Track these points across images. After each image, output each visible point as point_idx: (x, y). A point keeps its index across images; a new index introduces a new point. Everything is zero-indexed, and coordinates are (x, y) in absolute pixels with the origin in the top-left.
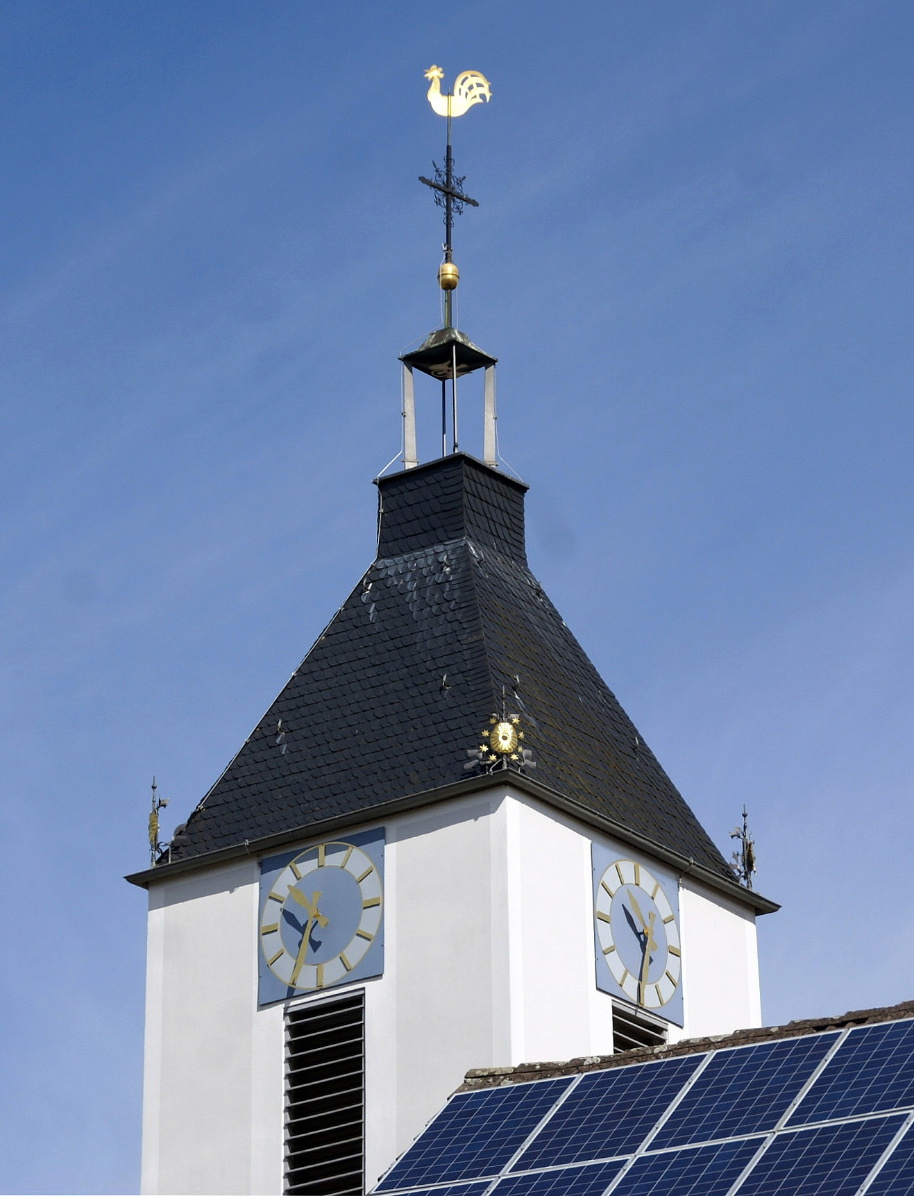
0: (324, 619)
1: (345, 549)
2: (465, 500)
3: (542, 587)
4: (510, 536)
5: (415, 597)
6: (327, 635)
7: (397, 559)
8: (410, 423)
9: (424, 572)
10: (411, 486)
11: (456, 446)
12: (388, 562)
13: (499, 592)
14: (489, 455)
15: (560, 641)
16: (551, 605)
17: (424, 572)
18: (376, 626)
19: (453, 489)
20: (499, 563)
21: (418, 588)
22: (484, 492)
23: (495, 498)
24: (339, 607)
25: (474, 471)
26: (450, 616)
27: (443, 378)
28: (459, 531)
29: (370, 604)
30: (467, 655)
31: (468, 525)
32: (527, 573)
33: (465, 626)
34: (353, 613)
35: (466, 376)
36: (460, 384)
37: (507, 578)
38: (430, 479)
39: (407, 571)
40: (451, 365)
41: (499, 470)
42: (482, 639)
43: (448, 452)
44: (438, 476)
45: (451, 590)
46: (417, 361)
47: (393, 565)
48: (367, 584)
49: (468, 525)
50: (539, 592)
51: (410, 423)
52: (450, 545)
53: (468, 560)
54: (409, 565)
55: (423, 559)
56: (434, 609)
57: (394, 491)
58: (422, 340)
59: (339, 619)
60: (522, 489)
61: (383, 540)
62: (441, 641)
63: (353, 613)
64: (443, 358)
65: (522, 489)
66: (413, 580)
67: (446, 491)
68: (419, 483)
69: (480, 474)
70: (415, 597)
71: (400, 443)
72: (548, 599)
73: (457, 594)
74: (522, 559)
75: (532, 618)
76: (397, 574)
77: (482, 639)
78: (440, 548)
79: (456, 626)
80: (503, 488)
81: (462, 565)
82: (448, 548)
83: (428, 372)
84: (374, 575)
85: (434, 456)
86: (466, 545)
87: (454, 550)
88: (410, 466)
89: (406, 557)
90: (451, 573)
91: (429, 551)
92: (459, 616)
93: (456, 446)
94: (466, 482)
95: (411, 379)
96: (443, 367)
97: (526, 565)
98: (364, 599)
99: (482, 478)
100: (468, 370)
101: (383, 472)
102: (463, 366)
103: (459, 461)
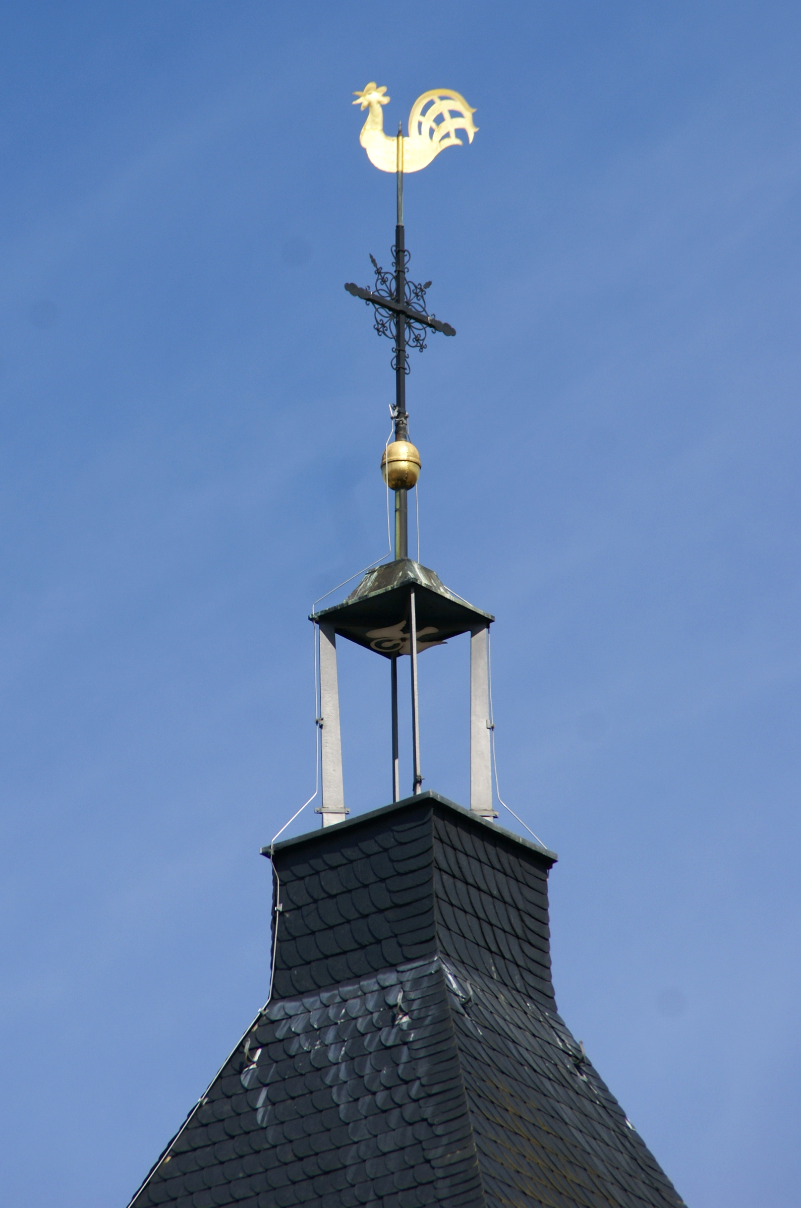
0: (170, 1122)
1: (216, 981)
2: (437, 886)
3: (588, 1052)
4: (521, 948)
5: (343, 1076)
6: (175, 1154)
7: (308, 1001)
8: (332, 739)
9: (361, 1025)
10: (334, 858)
11: (417, 781)
12: (291, 1006)
13: (502, 1062)
14: (480, 798)
15: (623, 1159)
16: (604, 1088)
17: (361, 1025)
18: (270, 1134)
19: (413, 864)
20: (502, 1006)
21: (349, 1058)
22: (471, 870)
23: (493, 881)
24: (196, 1095)
25: (452, 829)
26: (409, 1110)
27: (392, 653)
28: (425, 945)
29: (258, 1090)
30: (443, 1189)
31: (443, 933)
32: (557, 1025)
33: (439, 1130)
34: (226, 1108)
35: (436, 650)
36: (424, 663)
37: (517, 1034)
38: (370, 846)
39: (327, 1024)
40: (407, 629)
41: (499, 826)
42: (472, 1158)
43: (403, 793)
44: (386, 839)
45: (412, 1060)
46: (342, 622)
47: (303, 1013)
48: (253, 1050)
49: (443, 933)
50: (580, 1062)
51: (332, 739)
52: (409, 971)
53: (444, 1001)
54: (331, 1012)
55: (358, 1000)
56: (380, 1097)
57: (301, 869)
58: (355, 584)
59: (199, 1121)
60: (545, 862)
61: (282, 965)
62: (393, 1162)
63: (226, 1108)
64: (393, 617)
65: (545, 862)
66: (339, 1041)
67: (402, 867)
68: (350, 853)
69: (465, 835)
70: (343, 1076)
71: (313, 777)
72: (595, 1076)
73: (422, 1069)
74: (547, 997)
75: (567, 1113)
76: (309, 1030)
77: (472, 1158)
78: (390, 978)
79: (422, 1131)
80: (508, 859)
81: (433, 1011)
82: (408, 976)
83: (365, 643)
84: (264, 1032)
85: (377, 800)
86: (440, 971)
87: (417, 982)
88: (332, 820)
89: (325, 996)
90: (411, 1027)
91: (370, 984)
92: (428, 1112)
93: (417, 781)
94: (438, 852)
95: (331, 656)
96: (392, 633)
97: (554, 1009)
98: (245, 1080)
99: (468, 840)
100: (438, 639)
101: (284, 832)
102: (430, 630)
103: (424, 811)
